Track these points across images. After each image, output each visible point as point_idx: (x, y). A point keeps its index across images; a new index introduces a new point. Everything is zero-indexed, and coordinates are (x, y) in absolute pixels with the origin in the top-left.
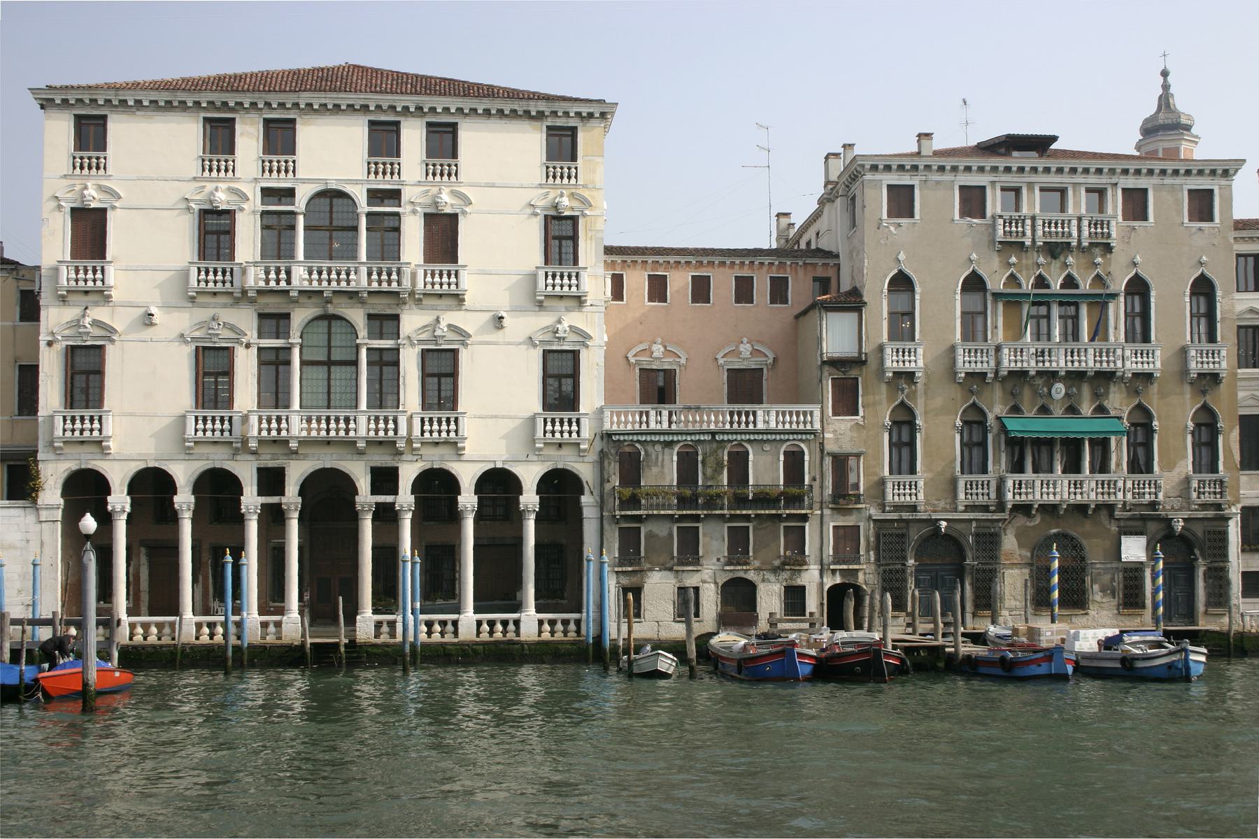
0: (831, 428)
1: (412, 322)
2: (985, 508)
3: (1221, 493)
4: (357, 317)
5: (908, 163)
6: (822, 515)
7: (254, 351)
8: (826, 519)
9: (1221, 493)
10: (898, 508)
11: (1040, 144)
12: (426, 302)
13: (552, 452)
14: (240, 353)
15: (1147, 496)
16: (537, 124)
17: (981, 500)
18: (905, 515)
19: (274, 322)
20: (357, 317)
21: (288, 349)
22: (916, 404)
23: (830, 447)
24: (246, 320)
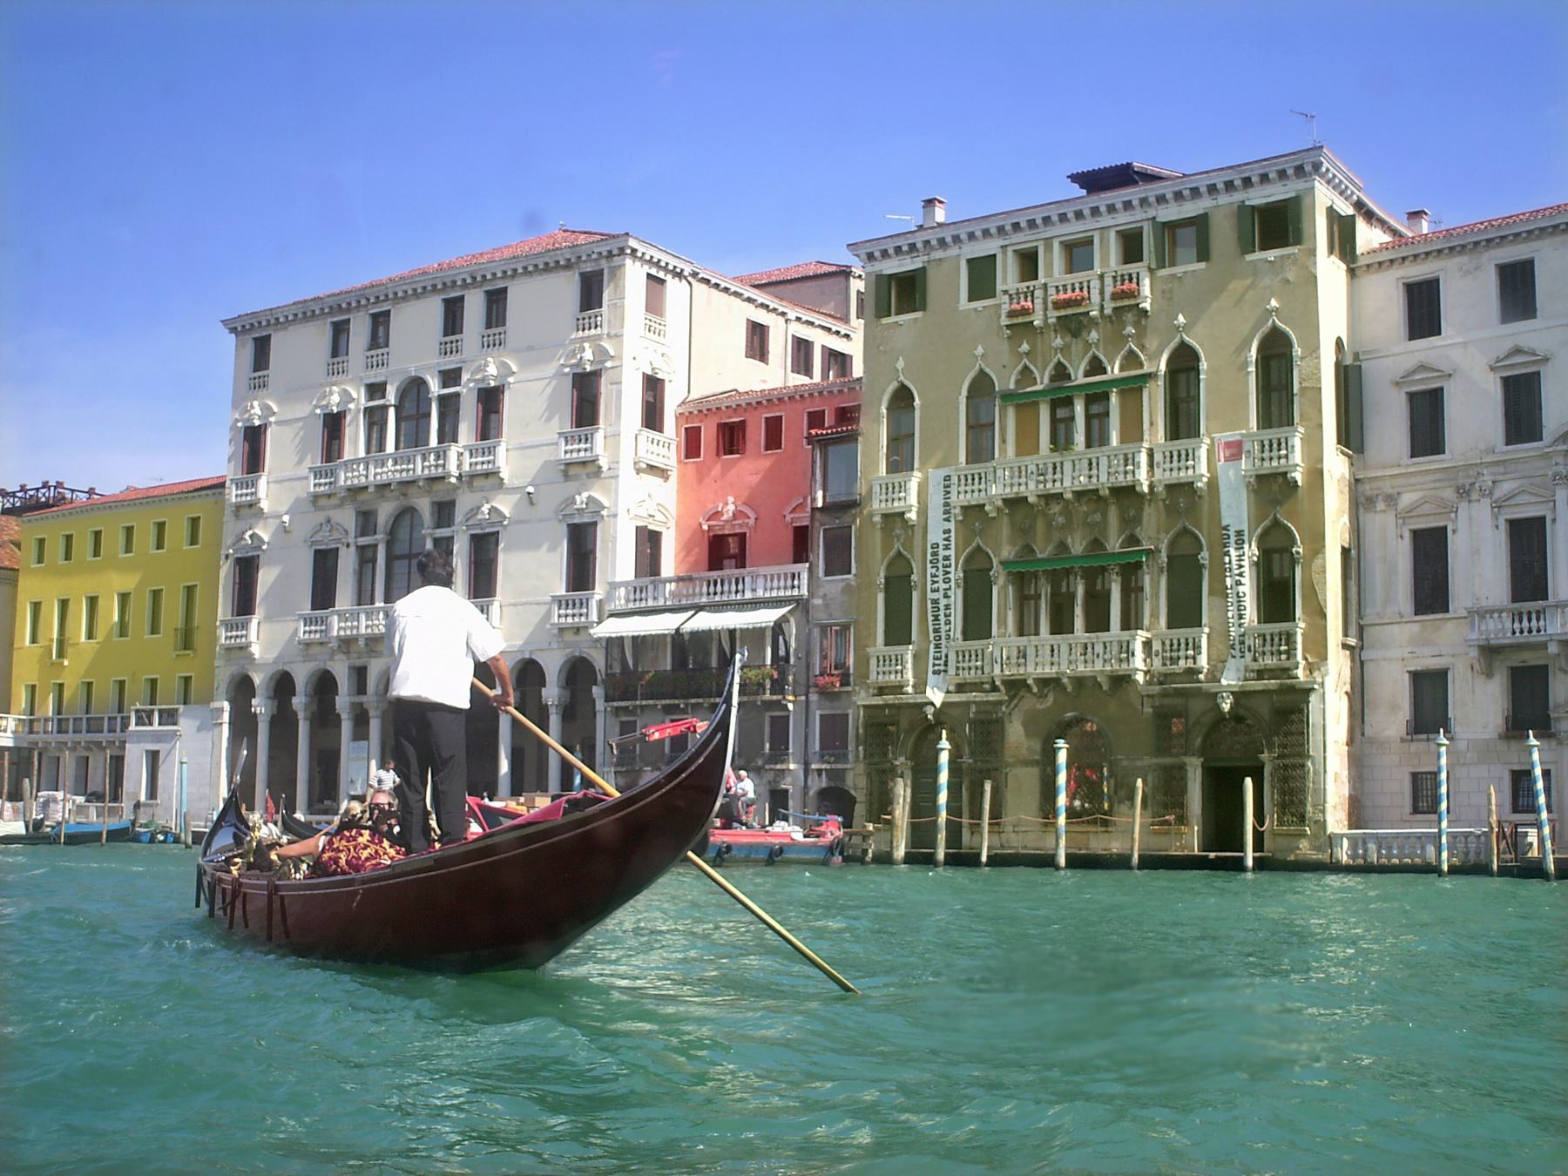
0: (821, 592)
1: (464, 503)
2: (976, 687)
3: (1287, 652)
4: (424, 505)
5: (992, 226)
6: (807, 701)
7: (353, 549)
8: (813, 706)
9: (1287, 652)
10: (881, 690)
11: (1123, 176)
12: (478, 483)
13: (569, 637)
14: (343, 552)
15: (1182, 662)
16: (569, 273)
17: (971, 676)
18: (890, 699)
19: (366, 521)
20: (424, 505)
21: (376, 546)
22: (912, 553)
23: (821, 616)
24: (347, 518)
